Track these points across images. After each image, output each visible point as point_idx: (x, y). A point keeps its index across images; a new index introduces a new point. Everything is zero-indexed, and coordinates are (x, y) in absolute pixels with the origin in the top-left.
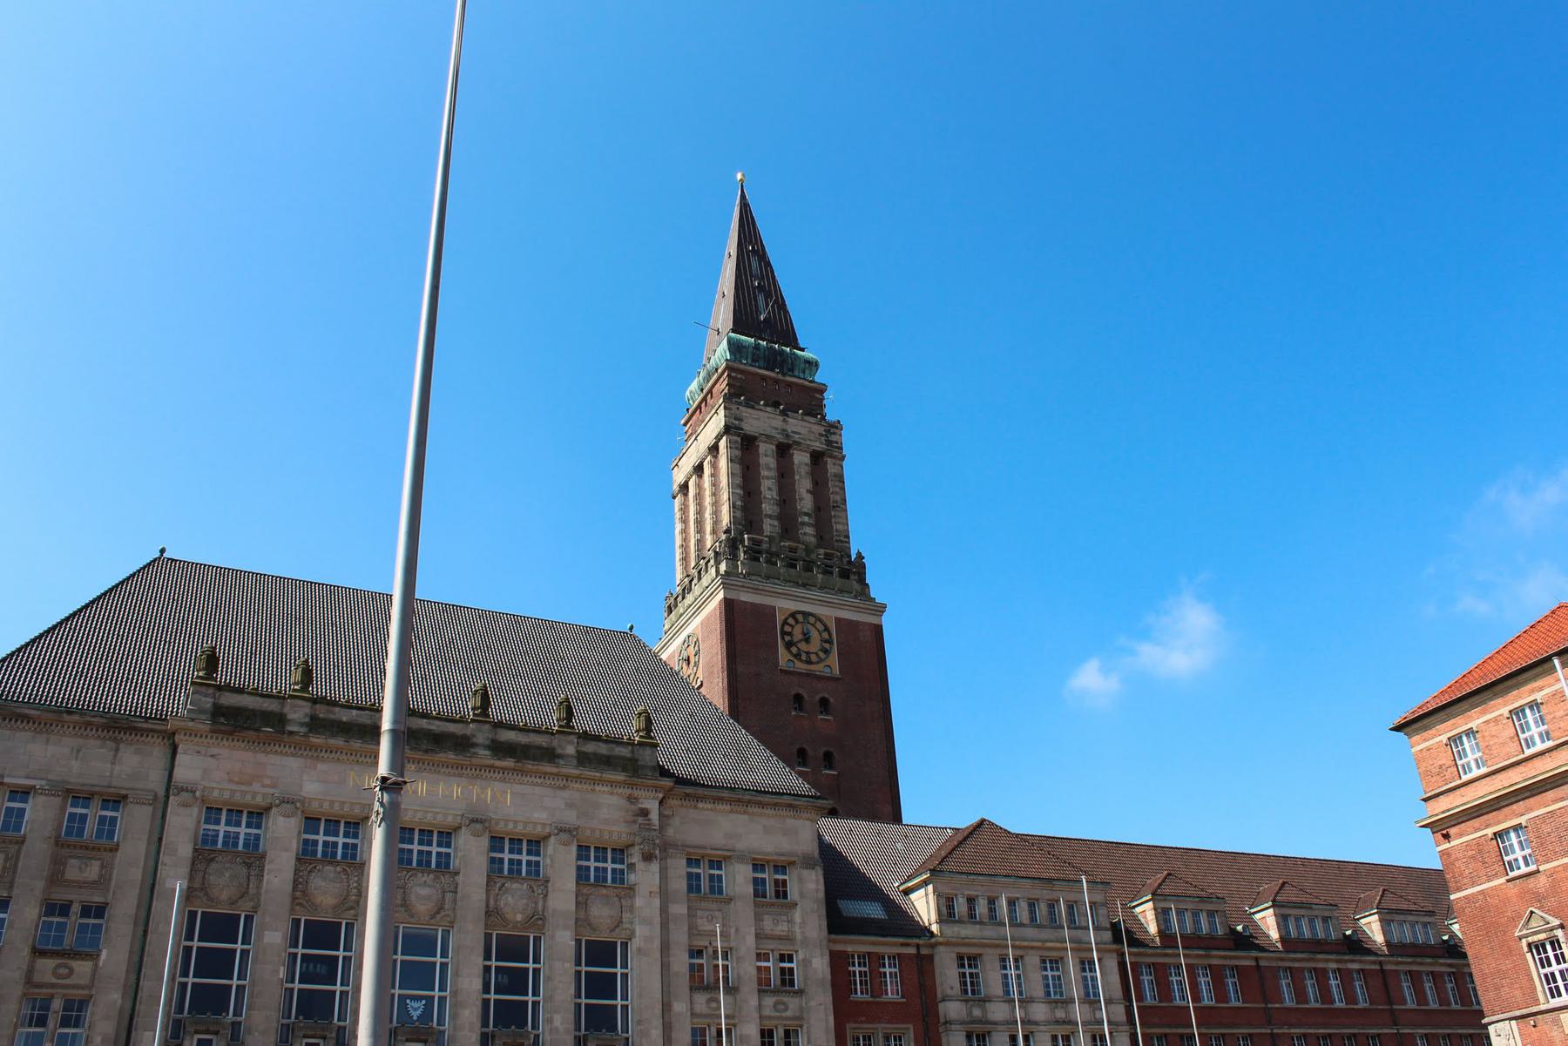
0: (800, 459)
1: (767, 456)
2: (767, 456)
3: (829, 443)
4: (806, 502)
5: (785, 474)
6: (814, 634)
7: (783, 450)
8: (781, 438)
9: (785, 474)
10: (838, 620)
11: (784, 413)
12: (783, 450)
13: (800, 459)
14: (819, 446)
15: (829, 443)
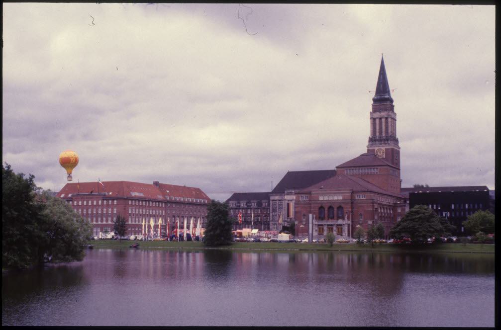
0: (383, 120)
1: (377, 121)
2: (377, 121)
3: (388, 115)
4: (384, 127)
5: (381, 123)
6: (381, 152)
7: (381, 119)
8: (379, 117)
9: (381, 123)
10: (386, 149)
11: (380, 112)
12: (381, 119)
13: (383, 120)
14: (386, 116)
15: (388, 115)
